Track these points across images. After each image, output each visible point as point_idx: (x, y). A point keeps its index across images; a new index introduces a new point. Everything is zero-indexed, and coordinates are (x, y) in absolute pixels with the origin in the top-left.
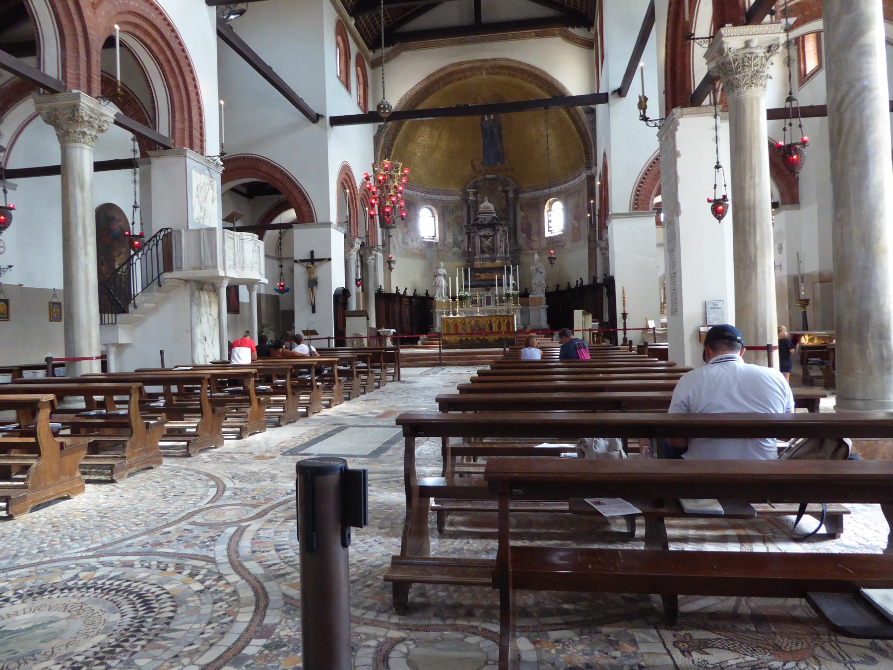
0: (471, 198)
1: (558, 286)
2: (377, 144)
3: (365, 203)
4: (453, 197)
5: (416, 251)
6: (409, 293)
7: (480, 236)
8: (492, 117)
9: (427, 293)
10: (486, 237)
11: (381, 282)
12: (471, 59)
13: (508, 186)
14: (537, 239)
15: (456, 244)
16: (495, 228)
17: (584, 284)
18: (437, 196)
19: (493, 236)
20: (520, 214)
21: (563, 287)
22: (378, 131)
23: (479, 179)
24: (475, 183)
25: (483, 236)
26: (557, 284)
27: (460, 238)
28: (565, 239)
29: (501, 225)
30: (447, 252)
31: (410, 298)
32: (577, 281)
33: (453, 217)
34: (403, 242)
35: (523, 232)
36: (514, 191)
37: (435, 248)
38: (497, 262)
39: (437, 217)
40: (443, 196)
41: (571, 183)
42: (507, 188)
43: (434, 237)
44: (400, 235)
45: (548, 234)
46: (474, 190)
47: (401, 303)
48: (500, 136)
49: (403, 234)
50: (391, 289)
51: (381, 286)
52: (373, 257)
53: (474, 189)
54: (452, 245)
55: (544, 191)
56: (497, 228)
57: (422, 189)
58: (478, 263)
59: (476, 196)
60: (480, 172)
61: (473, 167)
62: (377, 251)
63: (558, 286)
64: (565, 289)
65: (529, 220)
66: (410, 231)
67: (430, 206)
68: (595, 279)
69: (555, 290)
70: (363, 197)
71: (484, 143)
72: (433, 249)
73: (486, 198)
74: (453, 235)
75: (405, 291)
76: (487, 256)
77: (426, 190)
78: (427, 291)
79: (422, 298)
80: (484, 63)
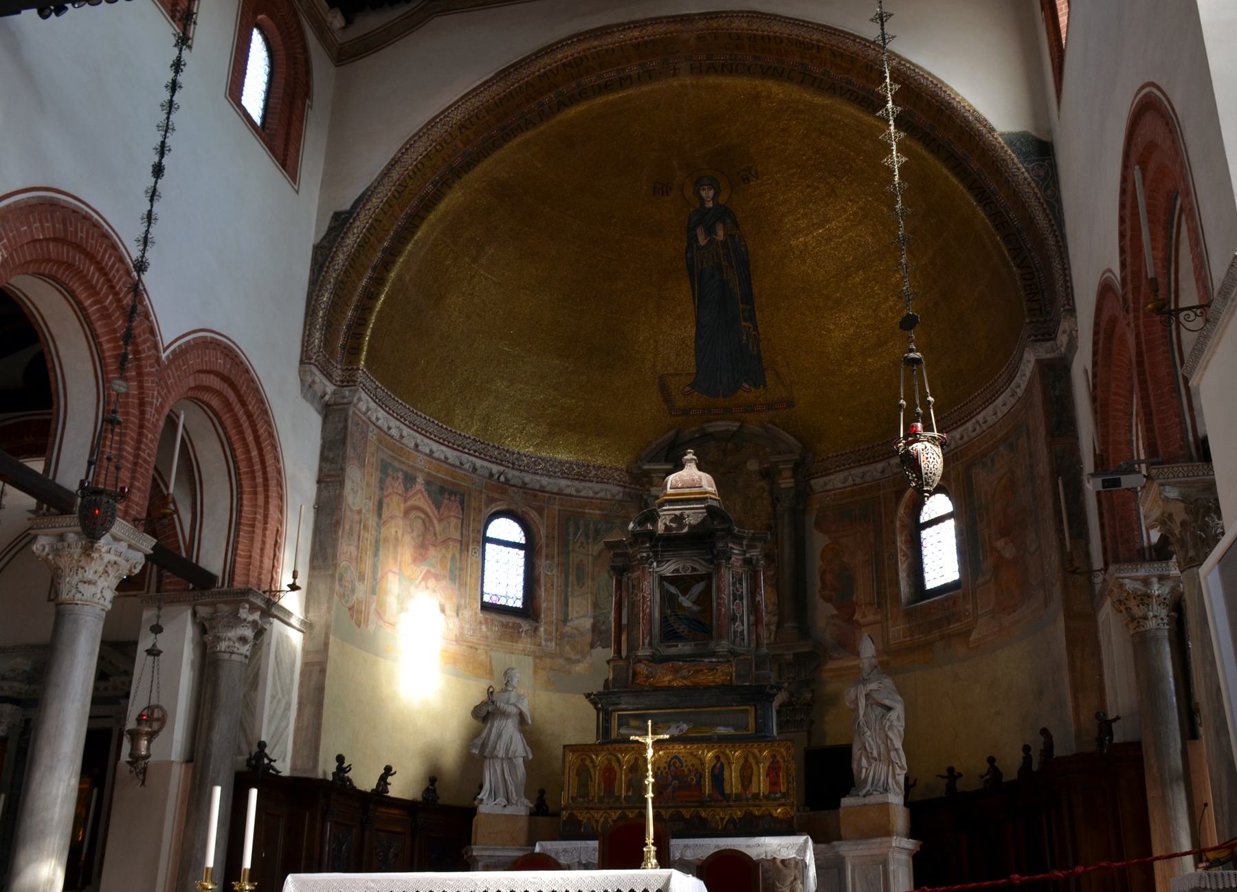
3: (232, 432)
4: (597, 487)
7: (663, 578)
8: (720, 235)
12: (639, 15)
17: (1058, 752)
18: (545, 481)
19: (708, 577)
22: (331, 229)
25: (673, 580)
29: (738, 539)
35: (828, 600)
40: (563, 483)
48: (748, 298)
54: (588, 637)
68: (1105, 726)
73: (689, 456)
74: (595, 605)
76: (683, 648)
80: (679, 26)
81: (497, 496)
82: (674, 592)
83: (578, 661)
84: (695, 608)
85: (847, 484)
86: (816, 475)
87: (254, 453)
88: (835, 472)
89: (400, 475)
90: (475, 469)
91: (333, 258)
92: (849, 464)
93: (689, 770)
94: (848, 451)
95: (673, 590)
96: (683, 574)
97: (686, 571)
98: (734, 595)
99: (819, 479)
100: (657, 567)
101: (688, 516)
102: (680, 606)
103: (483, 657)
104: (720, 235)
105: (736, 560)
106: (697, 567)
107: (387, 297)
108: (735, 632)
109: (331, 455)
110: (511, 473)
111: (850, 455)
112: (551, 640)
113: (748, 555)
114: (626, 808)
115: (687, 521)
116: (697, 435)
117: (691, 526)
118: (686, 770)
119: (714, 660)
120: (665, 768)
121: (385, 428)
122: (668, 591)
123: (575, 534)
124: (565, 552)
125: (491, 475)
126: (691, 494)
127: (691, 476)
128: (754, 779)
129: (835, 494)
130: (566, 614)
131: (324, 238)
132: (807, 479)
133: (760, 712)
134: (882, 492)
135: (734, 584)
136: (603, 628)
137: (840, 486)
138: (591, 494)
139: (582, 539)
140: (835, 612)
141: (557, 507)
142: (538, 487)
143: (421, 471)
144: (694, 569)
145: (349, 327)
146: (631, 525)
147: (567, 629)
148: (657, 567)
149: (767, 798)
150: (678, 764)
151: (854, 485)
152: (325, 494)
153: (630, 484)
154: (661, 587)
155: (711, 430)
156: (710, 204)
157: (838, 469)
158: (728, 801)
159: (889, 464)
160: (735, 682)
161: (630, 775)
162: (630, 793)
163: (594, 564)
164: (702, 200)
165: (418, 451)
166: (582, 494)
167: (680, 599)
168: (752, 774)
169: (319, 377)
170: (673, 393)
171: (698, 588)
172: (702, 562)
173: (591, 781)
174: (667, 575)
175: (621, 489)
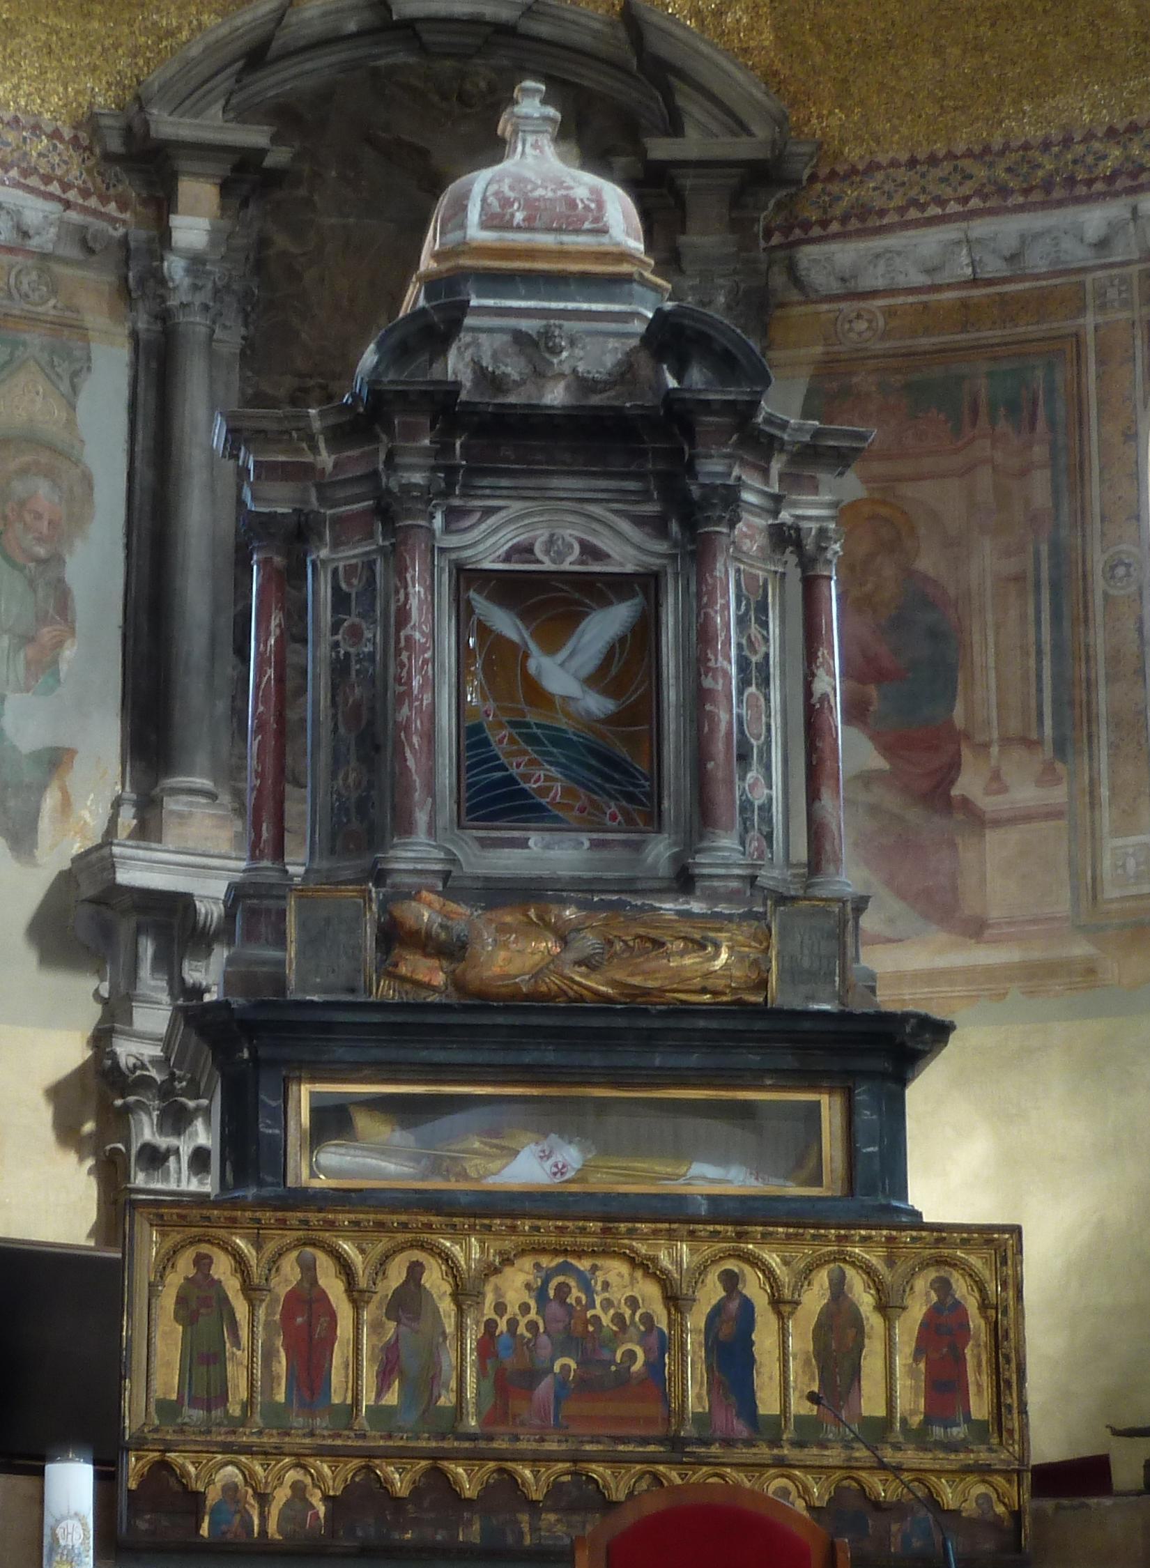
65: (927, 563)
82: (511, 634)
84: (597, 704)
85: (940, 279)
86: (816, 231)
88: (906, 225)
92: (965, 200)
93: (619, 1319)
94: (960, 148)
95: (505, 623)
96: (548, 566)
97: (560, 557)
98: (743, 665)
99: (834, 247)
100: (447, 530)
101: (572, 343)
102: (536, 693)
106: (604, 542)
108: (746, 806)
111: (966, 163)
113: (785, 516)
114: (389, 1455)
115: (564, 359)
116: (352, 27)
117: (584, 385)
118: (606, 1320)
119: (696, 907)
120: (525, 1308)
122: (484, 631)
126: (563, 254)
127: (560, 184)
128: (872, 1364)
129: (890, 312)
132: (776, 240)
133: (866, 1115)
134: (1090, 320)
135: (742, 621)
137: (920, 279)
140: (876, 761)
144: (591, 552)
146: (369, 358)
148: (447, 530)
149: (919, 1437)
150: (576, 1293)
151: (975, 282)
153: (85, 193)
154: (463, 611)
157: (913, 214)
158: (775, 1443)
159: (1135, 210)
160: (779, 995)
161: (392, 1325)
162: (392, 1398)
167: (532, 665)
168: (861, 1347)
172: (625, 526)
173: (237, 1343)
174: (487, 565)
175: (53, 208)
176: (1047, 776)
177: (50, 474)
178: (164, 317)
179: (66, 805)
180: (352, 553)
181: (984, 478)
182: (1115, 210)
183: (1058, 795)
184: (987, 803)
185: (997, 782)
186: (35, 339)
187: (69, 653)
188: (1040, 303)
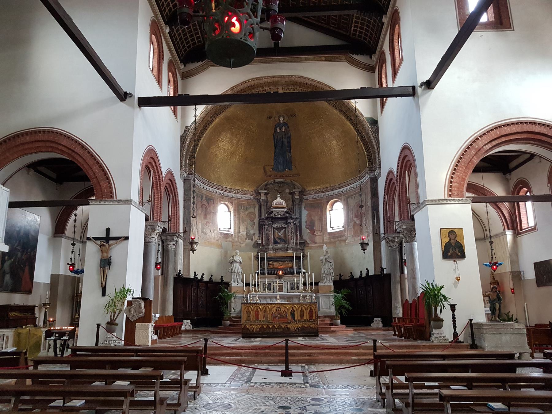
0: (263, 197)
1: (341, 276)
2: (183, 142)
4: (247, 196)
5: (213, 241)
6: (206, 278)
7: (274, 228)
8: (283, 129)
9: (222, 279)
10: (279, 229)
11: (180, 267)
13: (295, 189)
14: (319, 234)
15: (249, 236)
16: (287, 221)
18: (233, 195)
19: (285, 228)
20: (305, 213)
21: (347, 277)
22: (185, 131)
23: (270, 182)
24: (266, 185)
25: (276, 228)
26: (340, 274)
27: (252, 232)
28: (346, 234)
29: (292, 219)
30: (240, 243)
31: (206, 282)
32: (361, 272)
33: (246, 213)
34: (203, 232)
35: (308, 228)
36: (299, 193)
37: (230, 239)
38: (288, 252)
39: (232, 212)
40: (238, 195)
41: (352, 186)
42: (294, 190)
43: (229, 229)
44: (200, 226)
45: (329, 230)
46: (266, 191)
47: (198, 287)
48: (290, 146)
49: (203, 225)
50: (189, 275)
51: (180, 271)
52: (175, 243)
53: (265, 190)
55: (326, 193)
56: (289, 221)
57: (220, 187)
58: (271, 252)
59: (266, 197)
60: (270, 176)
61: (265, 172)
62: (178, 238)
63: (341, 276)
64: (348, 278)
66: (209, 223)
67: (227, 203)
69: (338, 280)
70: (167, 186)
71: (275, 152)
72: (228, 240)
73: (279, 195)
74: (247, 228)
75: (202, 276)
76: (280, 246)
77: (225, 189)
78: (222, 277)
79: (217, 283)
81: (222, 199)
83: (243, 243)
87: (174, 197)
89: (200, 196)
90: (216, 192)
91: (186, 140)
103: (220, 243)
104: (283, 129)
105: (292, 224)
106: (283, 225)
107: (199, 149)
109: (187, 193)
110: (225, 193)
112: (236, 238)
117: (281, 215)
121: (197, 184)
123: (241, 209)
124: (239, 214)
125: (220, 193)
130: (239, 231)
131: (183, 134)
136: (249, 234)
138: (245, 198)
139: (243, 211)
140: (309, 232)
141: (236, 202)
142: (231, 196)
143: (205, 194)
145: (189, 158)
147: (240, 235)
152: (186, 204)
154: (274, 230)
155: (277, 181)
156: (282, 122)
163: (246, 217)
164: (280, 120)
165: (203, 189)
166: (243, 198)
169: (185, 173)
170: (267, 171)
171: (283, 231)
176: (320, 233)
177: (253, 215)
178: (260, 203)
179: (255, 237)
180: (267, 227)
181: (316, 212)
182: (324, 194)
183: (321, 234)
184: (316, 234)
185: (317, 233)
186: (252, 206)
187: (255, 227)
188: (319, 200)
